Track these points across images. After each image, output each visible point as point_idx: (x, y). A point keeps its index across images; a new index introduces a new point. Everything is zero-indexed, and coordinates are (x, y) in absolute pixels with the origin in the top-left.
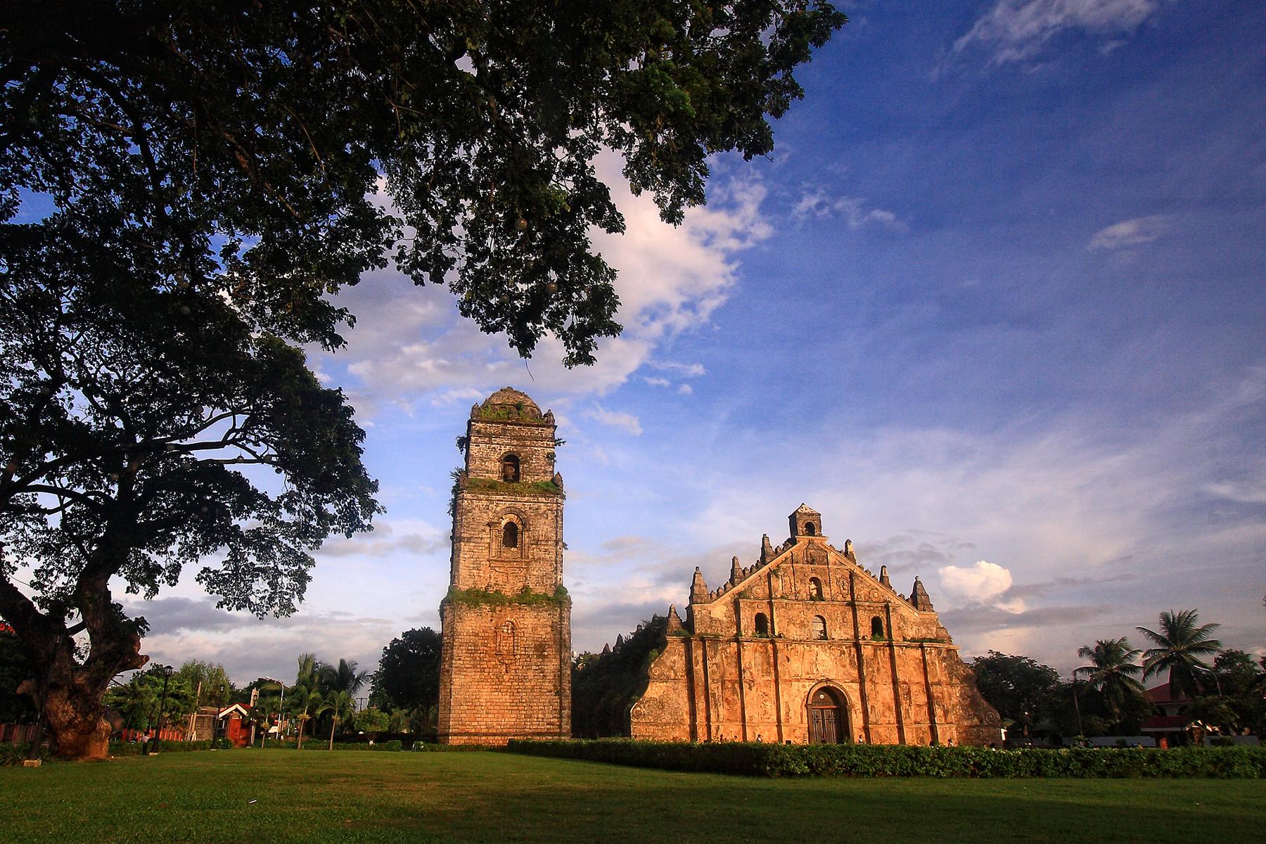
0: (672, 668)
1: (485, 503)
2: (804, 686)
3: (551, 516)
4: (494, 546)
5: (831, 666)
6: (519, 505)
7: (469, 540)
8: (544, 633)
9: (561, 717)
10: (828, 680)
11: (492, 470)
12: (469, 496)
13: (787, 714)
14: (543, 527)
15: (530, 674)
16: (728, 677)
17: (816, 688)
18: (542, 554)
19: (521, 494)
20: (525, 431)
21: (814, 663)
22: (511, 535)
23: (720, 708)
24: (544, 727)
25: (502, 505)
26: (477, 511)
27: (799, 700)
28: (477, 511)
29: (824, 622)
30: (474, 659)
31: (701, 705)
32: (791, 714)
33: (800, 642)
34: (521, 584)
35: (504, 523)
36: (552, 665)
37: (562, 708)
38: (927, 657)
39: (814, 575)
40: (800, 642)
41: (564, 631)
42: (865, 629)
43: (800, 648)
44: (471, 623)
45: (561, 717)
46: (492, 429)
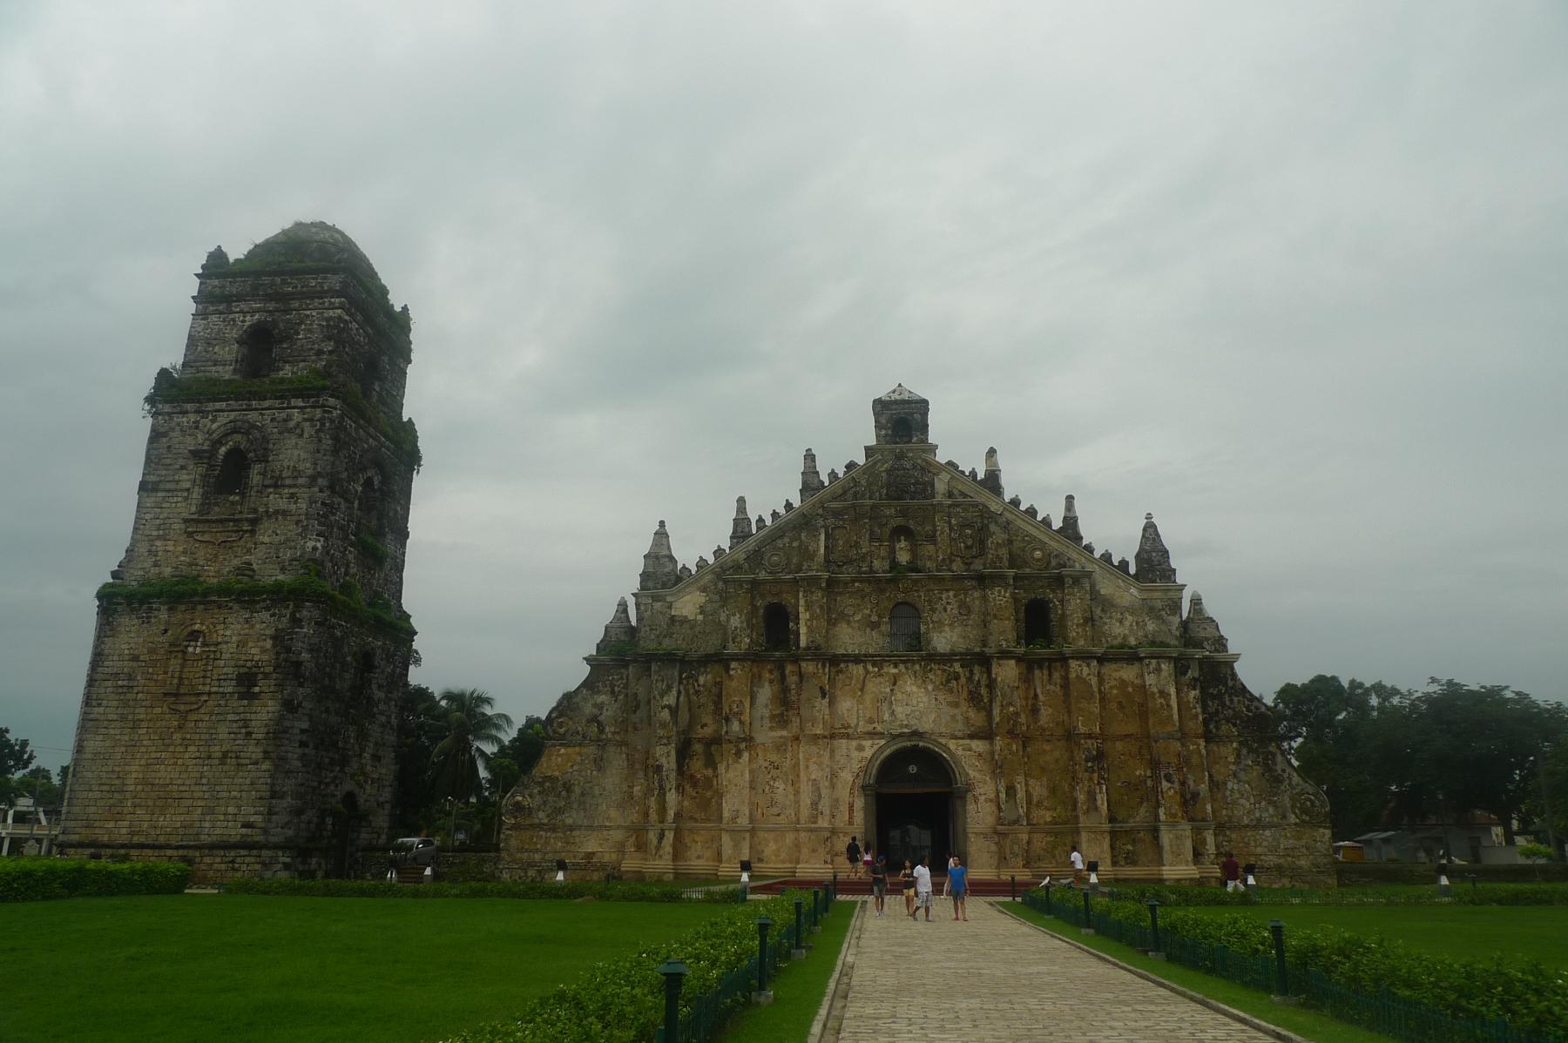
0: (594, 719)
1: (193, 417)
2: (860, 748)
3: (308, 430)
5: (920, 706)
6: (253, 416)
8: (259, 652)
9: (271, 813)
10: (915, 734)
12: (167, 408)
13: (815, 805)
18: (283, 504)
21: (887, 700)
23: (672, 797)
24: (236, 832)
25: (223, 419)
26: (177, 433)
27: (847, 777)
32: (825, 805)
33: (856, 659)
35: (223, 450)
36: (265, 711)
37: (274, 795)
38: (1150, 680)
39: (900, 521)
40: (856, 659)
43: (857, 670)
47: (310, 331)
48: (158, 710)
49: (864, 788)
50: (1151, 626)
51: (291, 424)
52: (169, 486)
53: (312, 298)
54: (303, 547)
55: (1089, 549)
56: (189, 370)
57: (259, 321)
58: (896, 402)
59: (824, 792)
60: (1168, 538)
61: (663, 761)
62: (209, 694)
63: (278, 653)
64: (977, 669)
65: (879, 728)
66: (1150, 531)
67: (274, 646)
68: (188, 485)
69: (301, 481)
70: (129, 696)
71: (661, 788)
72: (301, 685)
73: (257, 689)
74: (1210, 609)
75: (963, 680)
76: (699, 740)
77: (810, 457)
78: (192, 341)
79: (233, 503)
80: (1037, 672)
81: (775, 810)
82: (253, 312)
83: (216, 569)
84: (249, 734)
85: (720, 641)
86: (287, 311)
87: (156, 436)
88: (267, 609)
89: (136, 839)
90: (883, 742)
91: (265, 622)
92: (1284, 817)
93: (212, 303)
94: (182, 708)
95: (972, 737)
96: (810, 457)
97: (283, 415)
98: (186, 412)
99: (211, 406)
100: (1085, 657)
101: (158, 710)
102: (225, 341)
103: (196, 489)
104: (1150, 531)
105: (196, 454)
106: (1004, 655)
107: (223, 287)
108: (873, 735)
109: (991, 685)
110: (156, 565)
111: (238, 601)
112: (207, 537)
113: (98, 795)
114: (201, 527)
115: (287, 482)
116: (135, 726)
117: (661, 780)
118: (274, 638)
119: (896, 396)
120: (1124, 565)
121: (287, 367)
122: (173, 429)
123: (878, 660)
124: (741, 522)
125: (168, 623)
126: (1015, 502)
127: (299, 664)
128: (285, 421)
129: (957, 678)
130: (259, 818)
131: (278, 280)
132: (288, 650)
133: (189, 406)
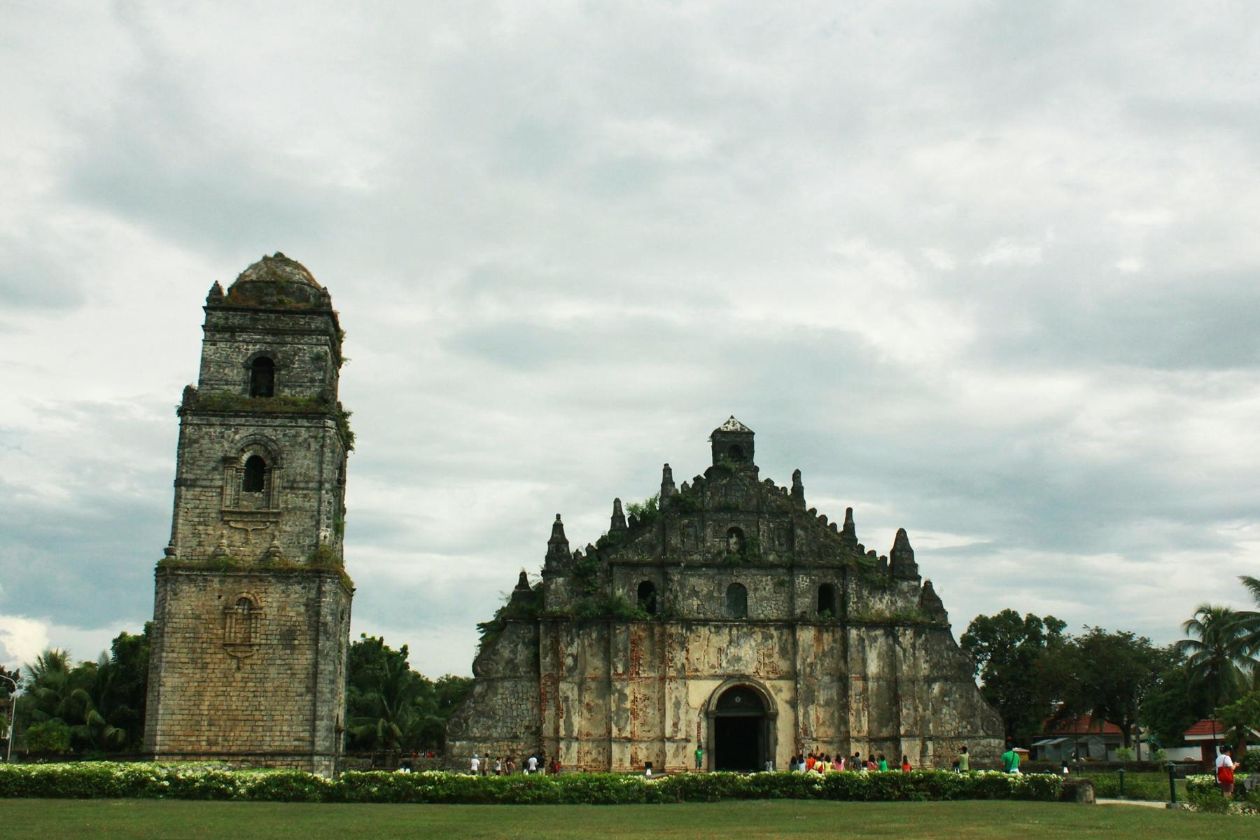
0: (510, 661)
3: (314, 446)
4: (229, 491)
6: (268, 432)
7: (192, 484)
11: (236, 379)
13: (675, 725)
14: (301, 462)
15: (273, 671)
16: (590, 672)
17: (724, 688)
18: (299, 502)
19: (272, 415)
20: (287, 322)
22: (257, 474)
23: (576, 720)
24: (290, 744)
28: (205, 441)
29: (746, 594)
30: (194, 651)
31: (549, 713)
32: (682, 725)
34: (266, 545)
35: (245, 457)
36: (303, 660)
40: (705, 622)
41: (324, 611)
42: (805, 603)
43: (704, 631)
44: (191, 601)
45: (314, 730)
46: (236, 320)
47: (304, 362)
48: (220, 656)
49: (707, 714)
50: (900, 604)
51: (300, 440)
52: (204, 483)
53: (303, 335)
54: (318, 536)
55: (862, 547)
56: (205, 387)
57: (260, 352)
58: (731, 432)
59: (682, 716)
60: (913, 544)
61: (569, 694)
62: (260, 645)
63: (310, 617)
64: (785, 631)
65: (719, 671)
66: (901, 536)
67: (307, 611)
68: (219, 483)
69: (311, 485)
70: (196, 645)
71: (568, 711)
72: (328, 639)
73: (296, 642)
74: (936, 588)
75: (775, 639)
76: (593, 679)
77: (667, 470)
78: (205, 363)
80: (825, 635)
81: (647, 728)
82: (255, 344)
83: (245, 547)
84: (293, 674)
85: (591, 601)
86: (284, 344)
87: (185, 443)
88: (299, 583)
89: (214, 749)
90: (719, 682)
91: (297, 591)
92: (977, 731)
93: (218, 332)
94: (239, 655)
95: (780, 678)
96: (667, 470)
97: (293, 432)
98: (212, 425)
99: (232, 421)
100: (859, 624)
101: (220, 656)
102: (233, 365)
104: (901, 536)
106: (805, 622)
107: (227, 319)
108: (714, 677)
109: (795, 643)
110: (200, 544)
111: (274, 576)
112: (240, 525)
113: (180, 717)
114: (235, 517)
115: (302, 485)
116: (204, 667)
117: (567, 707)
118: (307, 605)
119: (730, 427)
120: (884, 558)
121: (286, 390)
122: (203, 438)
123: (719, 624)
124: (617, 517)
125: (221, 591)
126: (813, 511)
127: (325, 624)
128: (295, 436)
129: (772, 637)
130: (307, 734)
131: (273, 316)
132: (318, 614)
133: (213, 420)
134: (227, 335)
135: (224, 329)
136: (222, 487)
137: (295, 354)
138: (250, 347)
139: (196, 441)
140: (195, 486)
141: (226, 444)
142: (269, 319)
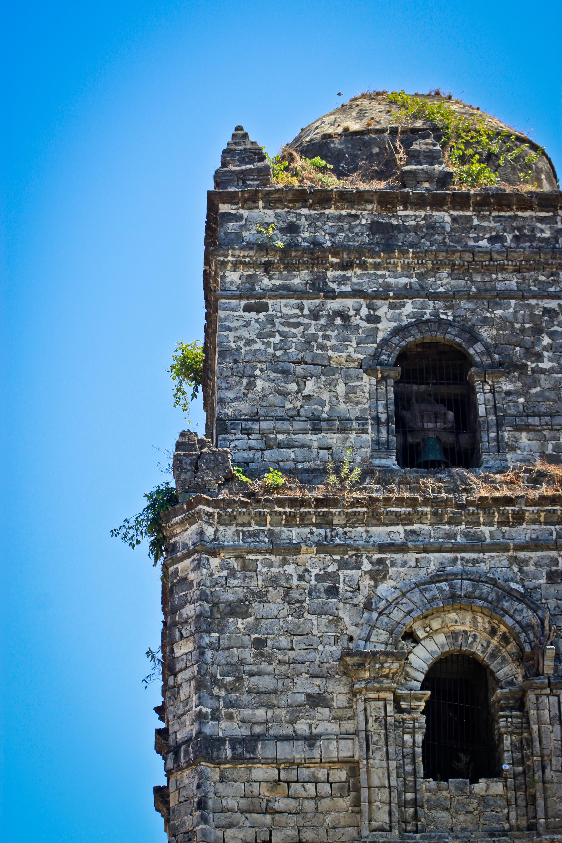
35: (421, 658)
52: (284, 751)
57: (419, 323)
68: (347, 749)
79: (483, 799)
93: (267, 267)
103: (378, 758)
105: (354, 662)
131: (444, 217)
133: (294, 534)
134: (300, 279)
135: (290, 258)
136: (352, 766)
137: (538, 331)
138: (385, 307)
139: (238, 609)
140: (253, 760)
141: (346, 615)
142: (432, 227)
